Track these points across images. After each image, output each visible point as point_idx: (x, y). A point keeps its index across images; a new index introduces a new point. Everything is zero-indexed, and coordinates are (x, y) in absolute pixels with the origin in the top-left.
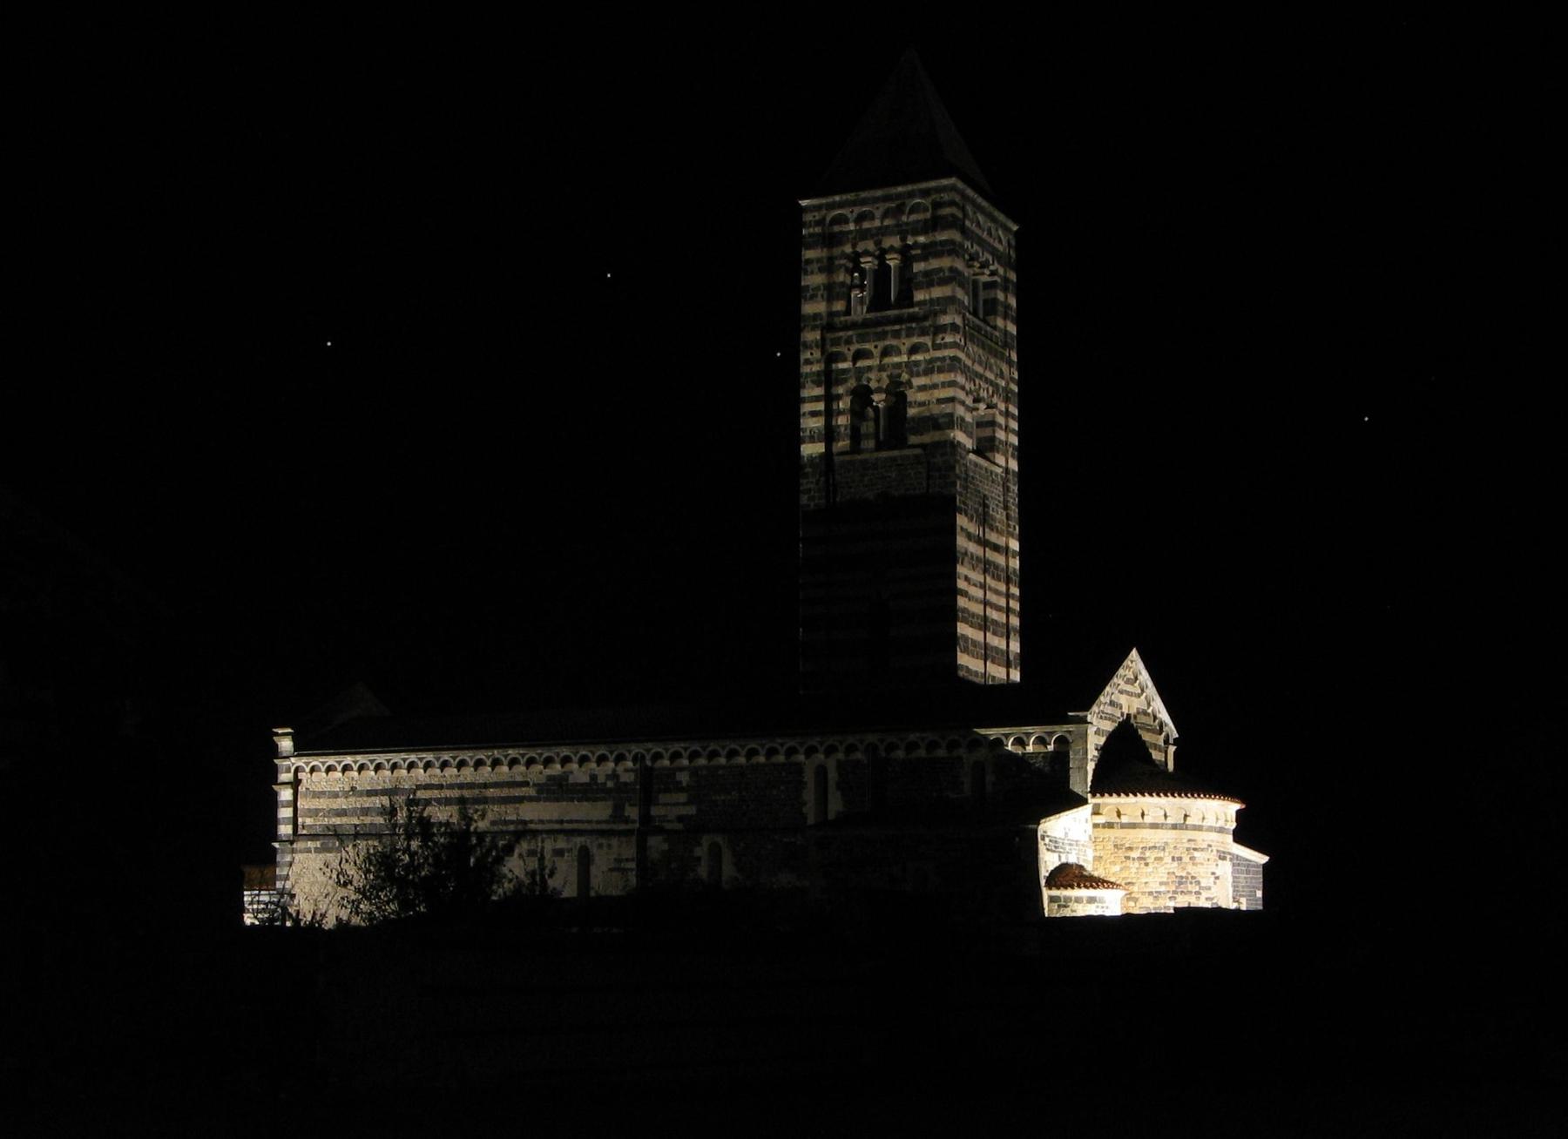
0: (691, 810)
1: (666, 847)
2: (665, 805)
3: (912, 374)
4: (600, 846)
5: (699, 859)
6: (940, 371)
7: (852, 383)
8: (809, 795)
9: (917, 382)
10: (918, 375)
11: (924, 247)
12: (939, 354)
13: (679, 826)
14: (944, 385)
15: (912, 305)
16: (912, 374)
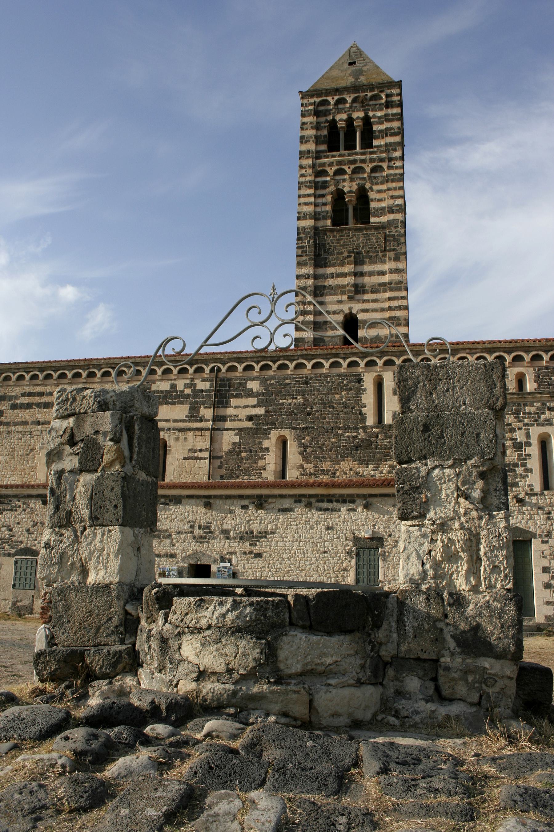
0: (261, 411)
1: (237, 439)
2: (236, 407)
3: (373, 184)
4: (177, 439)
5: (267, 449)
6: (393, 181)
7: (332, 188)
8: (368, 398)
9: (375, 188)
10: (377, 184)
11: (379, 118)
12: (392, 172)
13: (250, 424)
14: (395, 189)
15: (372, 147)
16: (373, 184)
